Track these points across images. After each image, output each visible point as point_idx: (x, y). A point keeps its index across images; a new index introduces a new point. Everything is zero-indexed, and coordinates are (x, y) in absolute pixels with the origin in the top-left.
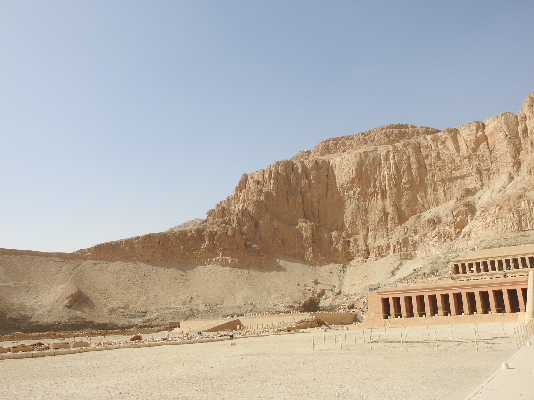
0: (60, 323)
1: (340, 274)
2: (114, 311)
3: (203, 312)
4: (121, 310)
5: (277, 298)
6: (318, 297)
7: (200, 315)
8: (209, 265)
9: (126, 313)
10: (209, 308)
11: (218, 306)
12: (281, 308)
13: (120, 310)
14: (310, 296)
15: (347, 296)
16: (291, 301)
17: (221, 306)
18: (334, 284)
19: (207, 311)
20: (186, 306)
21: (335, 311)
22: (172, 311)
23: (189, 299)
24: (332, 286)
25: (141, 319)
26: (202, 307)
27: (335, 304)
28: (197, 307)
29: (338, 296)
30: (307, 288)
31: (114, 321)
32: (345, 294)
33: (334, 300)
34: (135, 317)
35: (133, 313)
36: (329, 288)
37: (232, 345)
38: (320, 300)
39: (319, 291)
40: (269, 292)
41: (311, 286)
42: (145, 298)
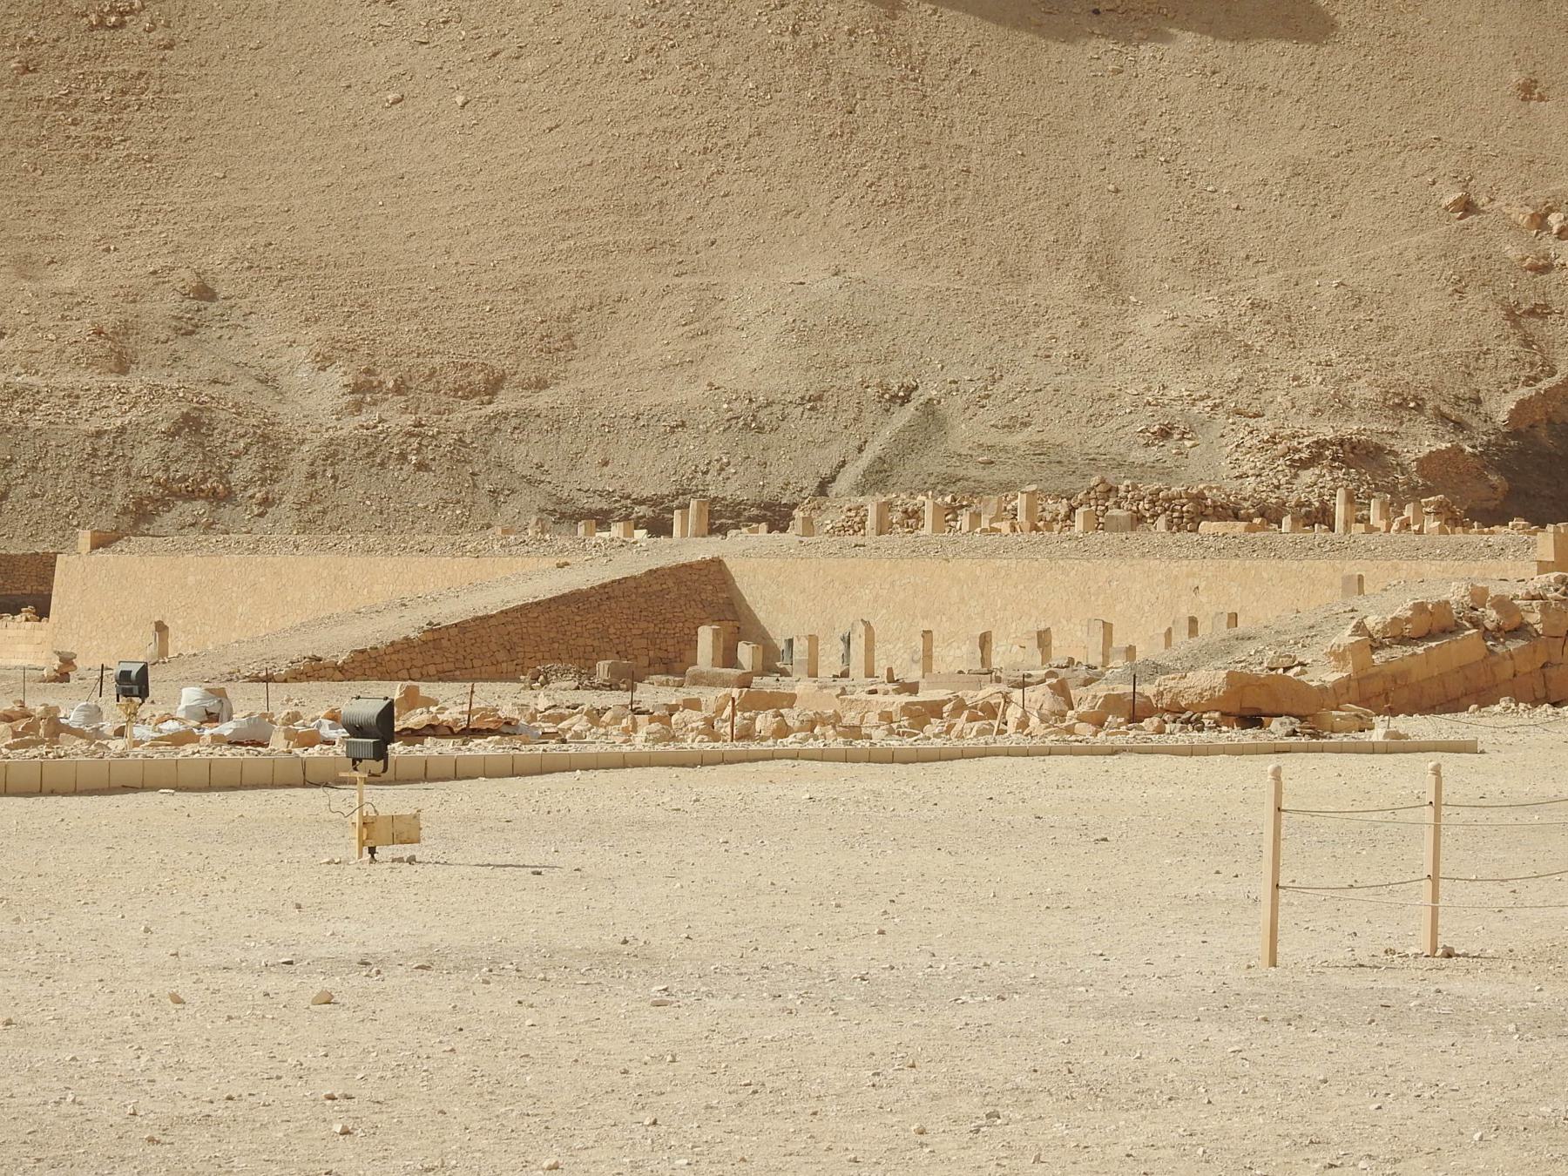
5: (1198, 345)
7: (293, 485)
10: (393, 416)
11: (506, 401)
12: (1225, 462)
16: (1363, 390)
17: (542, 400)
19: (373, 452)
20: (136, 382)
23: (166, 304)
28: (266, 400)
37: (375, 836)
40: (1109, 277)
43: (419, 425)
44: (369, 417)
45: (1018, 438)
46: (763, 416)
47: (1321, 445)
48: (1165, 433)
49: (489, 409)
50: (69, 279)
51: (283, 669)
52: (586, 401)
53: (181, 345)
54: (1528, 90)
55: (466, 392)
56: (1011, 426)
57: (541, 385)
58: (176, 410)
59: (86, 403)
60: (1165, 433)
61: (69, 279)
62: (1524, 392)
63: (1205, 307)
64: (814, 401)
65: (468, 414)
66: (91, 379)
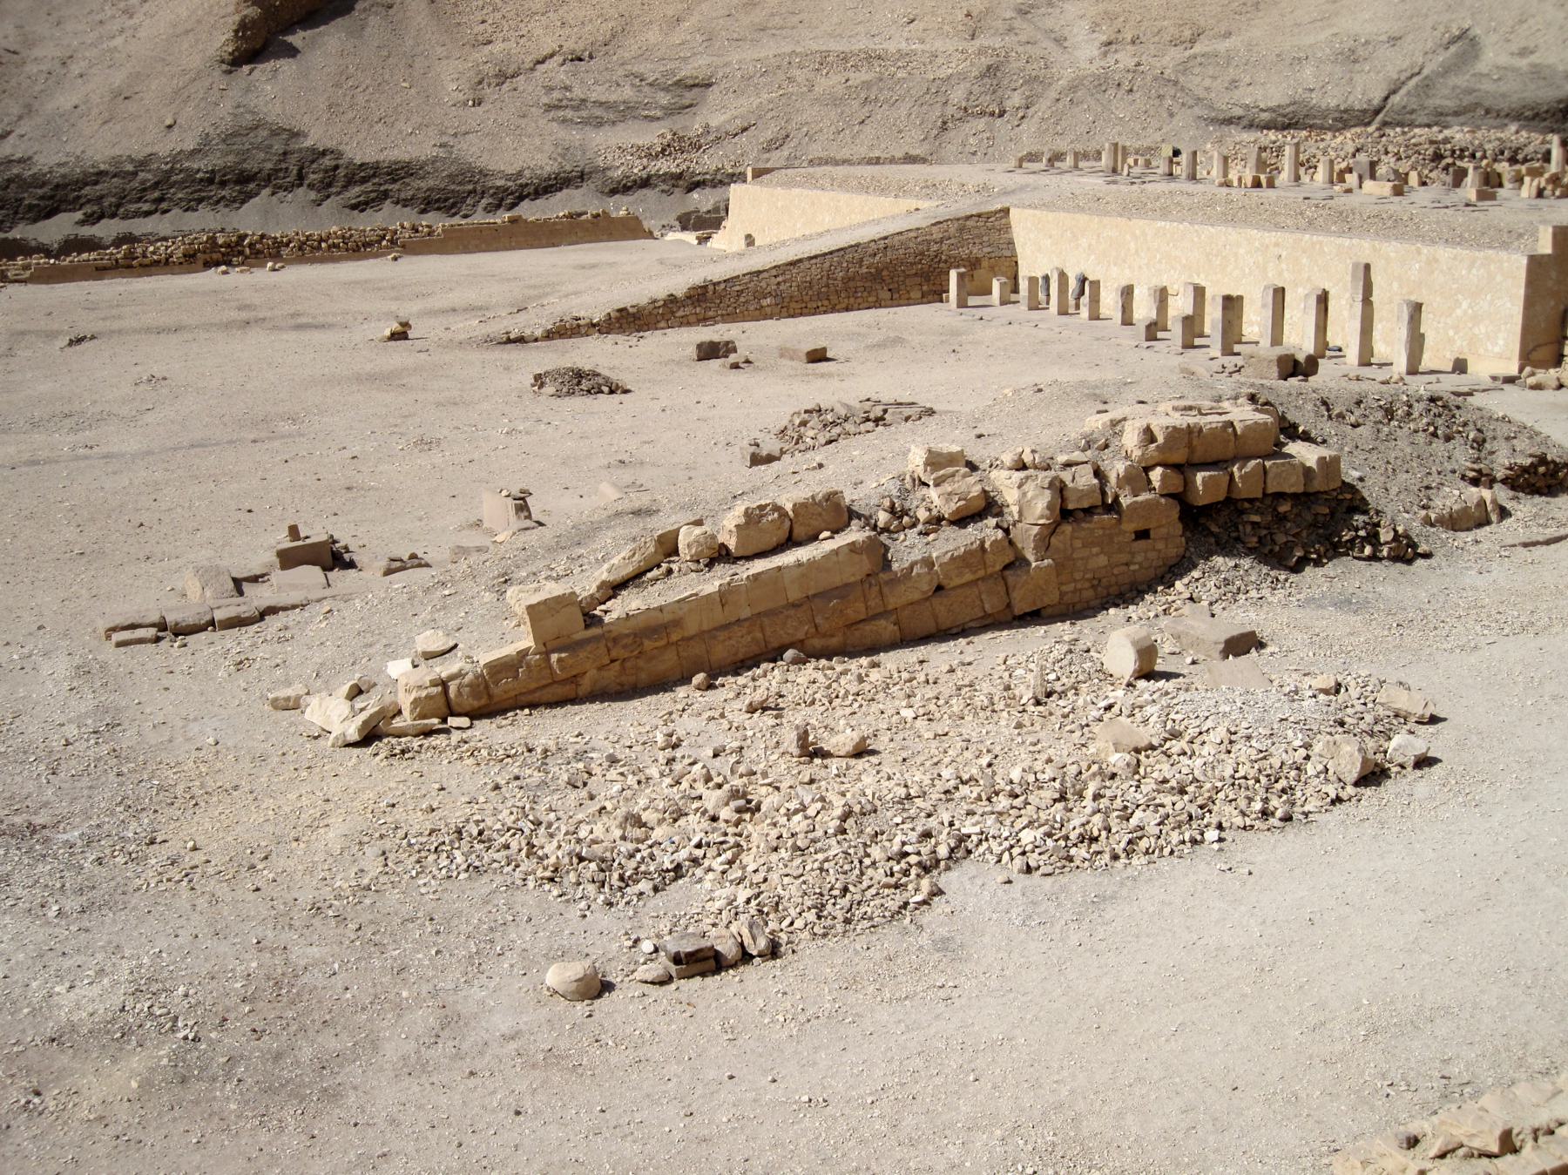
0: (143, 164)
2: (503, 77)
3: (1073, 88)
4: (555, 72)
9: (578, 92)
13: (555, 72)
17: (1223, 46)
25: (652, 136)
26: (1085, 53)
34: (625, 113)
35: (627, 93)
43: (1138, 64)
44: (1111, 60)
45: (1523, 63)
46: (1360, 52)
49: (1187, 53)
51: (539, 333)
52: (1250, 47)
53: (1017, 23)
55: (1174, 43)
56: (1524, 52)
57: (1228, 35)
58: (985, 61)
59: (940, 60)
64: (1394, 40)
65: (1176, 55)
66: (950, 46)
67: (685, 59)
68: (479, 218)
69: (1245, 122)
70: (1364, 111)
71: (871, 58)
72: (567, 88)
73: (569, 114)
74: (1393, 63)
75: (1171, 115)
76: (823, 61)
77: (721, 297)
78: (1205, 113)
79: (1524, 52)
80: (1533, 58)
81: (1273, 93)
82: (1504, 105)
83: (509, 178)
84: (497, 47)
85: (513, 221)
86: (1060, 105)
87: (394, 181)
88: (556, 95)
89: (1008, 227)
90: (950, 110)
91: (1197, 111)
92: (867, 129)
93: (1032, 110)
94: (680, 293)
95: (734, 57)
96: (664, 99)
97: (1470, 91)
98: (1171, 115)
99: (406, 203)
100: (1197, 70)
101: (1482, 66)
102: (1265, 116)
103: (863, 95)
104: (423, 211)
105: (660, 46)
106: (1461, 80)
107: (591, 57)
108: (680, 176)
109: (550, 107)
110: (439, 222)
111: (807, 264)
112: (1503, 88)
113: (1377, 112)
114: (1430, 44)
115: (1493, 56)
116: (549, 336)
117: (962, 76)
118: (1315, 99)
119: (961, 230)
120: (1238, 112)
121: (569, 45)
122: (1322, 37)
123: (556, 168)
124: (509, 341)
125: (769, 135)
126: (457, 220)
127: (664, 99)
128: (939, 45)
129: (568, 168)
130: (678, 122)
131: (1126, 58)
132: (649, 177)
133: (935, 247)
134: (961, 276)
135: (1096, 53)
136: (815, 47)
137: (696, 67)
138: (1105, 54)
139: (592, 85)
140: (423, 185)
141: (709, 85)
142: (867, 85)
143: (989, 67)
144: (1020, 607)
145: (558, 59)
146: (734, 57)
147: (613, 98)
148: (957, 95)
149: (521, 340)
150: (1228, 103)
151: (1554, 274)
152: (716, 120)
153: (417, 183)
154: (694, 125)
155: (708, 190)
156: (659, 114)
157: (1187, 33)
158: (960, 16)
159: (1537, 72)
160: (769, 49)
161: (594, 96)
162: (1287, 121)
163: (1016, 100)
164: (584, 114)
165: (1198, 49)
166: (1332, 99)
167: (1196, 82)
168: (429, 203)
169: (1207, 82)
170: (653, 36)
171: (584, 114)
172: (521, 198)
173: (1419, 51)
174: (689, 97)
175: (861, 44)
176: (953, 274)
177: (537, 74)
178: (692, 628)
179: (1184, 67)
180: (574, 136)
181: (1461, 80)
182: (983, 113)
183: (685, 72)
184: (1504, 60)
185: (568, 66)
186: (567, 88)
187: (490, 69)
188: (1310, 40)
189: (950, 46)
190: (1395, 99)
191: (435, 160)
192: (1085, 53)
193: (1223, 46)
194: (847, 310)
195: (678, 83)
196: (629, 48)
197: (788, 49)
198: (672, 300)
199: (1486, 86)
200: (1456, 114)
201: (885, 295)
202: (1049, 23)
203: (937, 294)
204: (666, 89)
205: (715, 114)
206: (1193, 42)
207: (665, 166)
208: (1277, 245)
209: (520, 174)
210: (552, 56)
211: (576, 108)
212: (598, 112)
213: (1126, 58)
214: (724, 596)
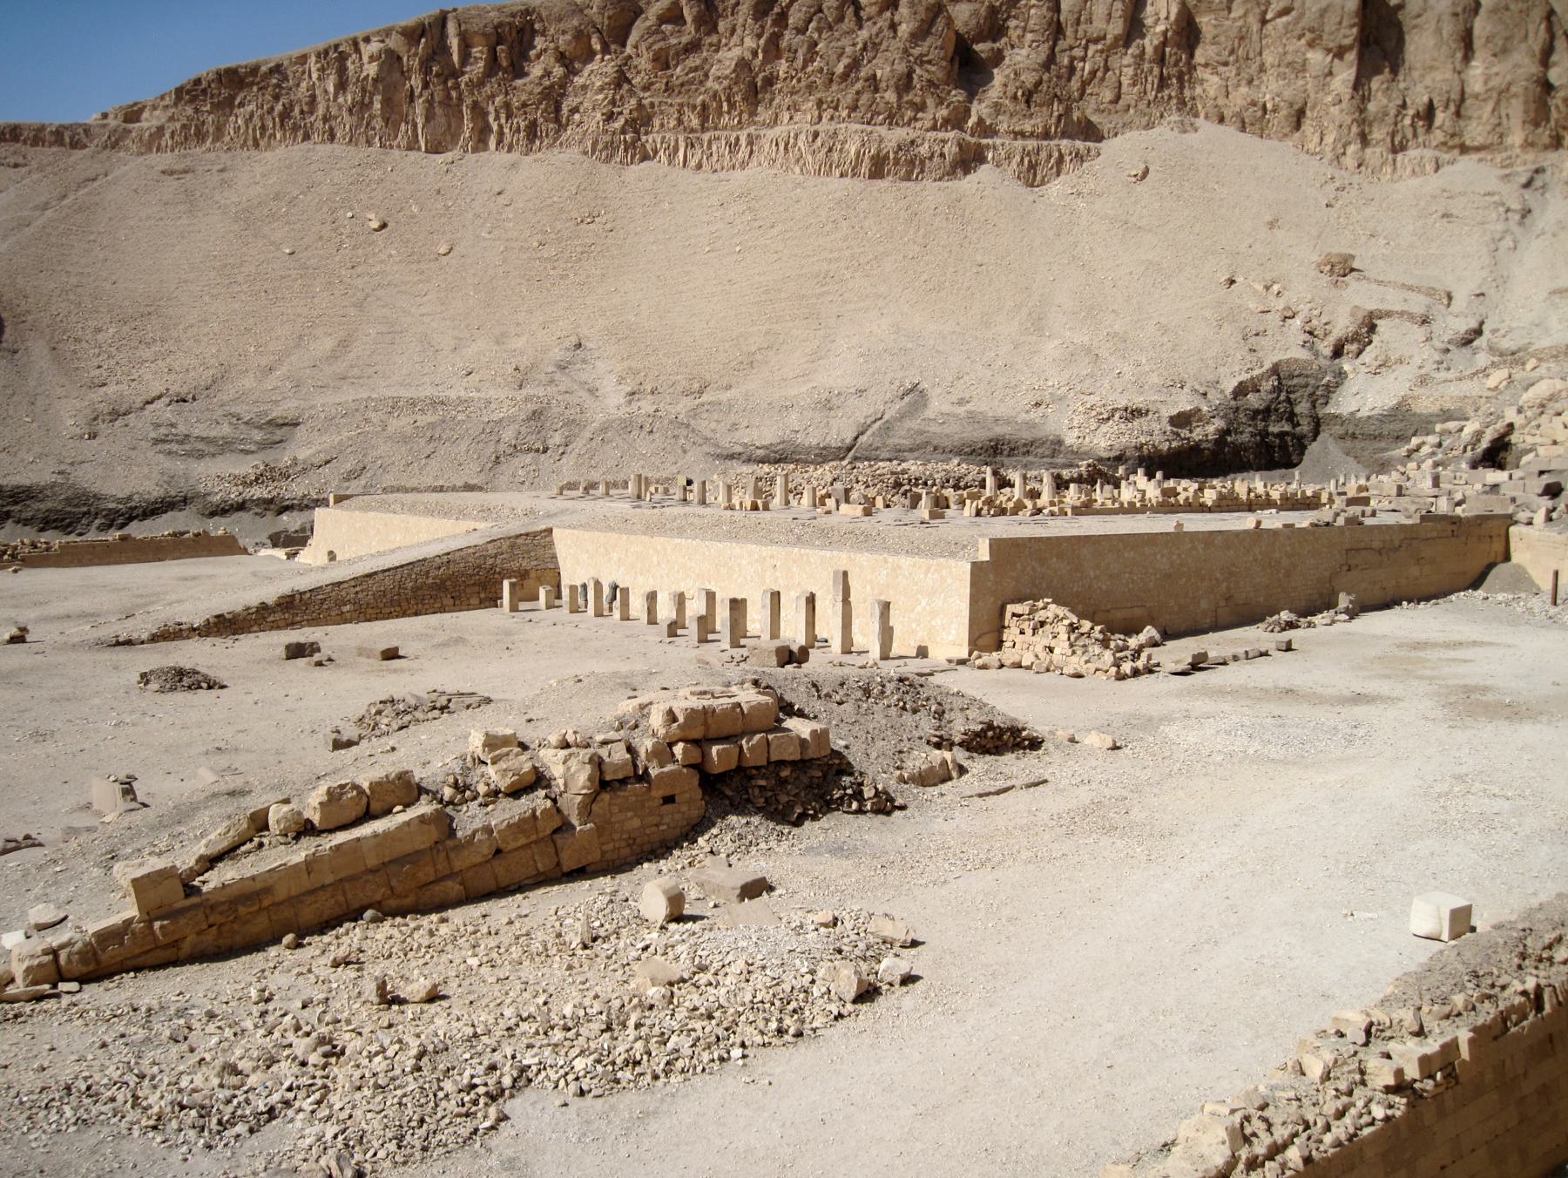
1: (1500, 227)
2: (115, 415)
3: (604, 429)
4: (163, 411)
6: (1338, 352)
8: (744, 165)
9: (182, 429)
14: (1287, 347)
15: (1514, 357)
16: (1155, 379)
17: (725, 396)
18: (1449, 283)
21: (1383, 467)
22: (423, 420)
24: (1431, 292)
25: (247, 467)
26: (613, 401)
27: (1426, 404)
29: (1457, 354)
30: (1280, 304)
31: (90, 478)
32: (1506, 344)
33: (1423, 381)
34: (224, 446)
35: (226, 430)
36: (1418, 304)
38: (1341, 375)
39: (1343, 325)
40: (1038, 324)
41: (1305, 289)
42: (328, 344)
44: (635, 406)
45: (961, 410)
46: (834, 401)
47: (1115, 410)
48: (1038, 404)
49: (697, 401)
50: (519, 343)
51: (145, 636)
52: (746, 397)
53: (558, 376)
54: (1272, 225)
56: (961, 402)
57: (729, 387)
58: (531, 407)
59: (493, 406)
60: (1038, 404)
61: (519, 343)
62: (1245, 377)
63: (1081, 338)
64: (861, 392)
65: (686, 404)
66: (502, 394)
67: (276, 402)
68: (93, 536)
69: (744, 457)
70: (839, 448)
71: (435, 403)
72: (172, 425)
73: (174, 447)
74: (861, 411)
75: (685, 452)
76: (395, 406)
77: (306, 605)
78: (711, 450)
79: (961, 402)
80: (968, 407)
81: (766, 435)
82: (947, 443)
83: (119, 501)
84: (111, 389)
85: (123, 539)
86: (593, 443)
87: (16, 503)
88: (163, 430)
89: (552, 544)
90: (502, 447)
91: (706, 449)
92: (433, 462)
93: (569, 449)
94: (271, 600)
95: (319, 401)
96: (258, 436)
97: (921, 433)
98: (685, 452)
99: (26, 522)
100: (705, 415)
101: (930, 413)
102: (761, 452)
103: (429, 434)
104: (42, 530)
105: (254, 391)
106: (914, 424)
107: (194, 399)
108: (271, 501)
109: (157, 441)
110: (56, 539)
111: (381, 576)
112: (947, 430)
113: (849, 449)
114: (889, 395)
115: (938, 405)
116: (154, 639)
117: (512, 419)
118: (800, 438)
119: (512, 546)
120: (738, 449)
121: (175, 389)
122: (804, 389)
123: (162, 493)
124: (118, 644)
125: (349, 467)
126: (72, 538)
127: (258, 436)
128: (492, 393)
129: (173, 493)
130: (270, 456)
131: (646, 405)
132: (244, 502)
133: (491, 561)
134: (512, 585)
135: (622, 401)
136: (388, 393)
137: (286, 408)
138: (630, 402)
139: (195, 423)
140: (42, 506)
141: (297, 424)
142: (432, 426)
143: (534, 412)
144: (567, 865)
145: (165, 400)
146: (319, 401)
147: (213, 434)
148: (508, 435)
149: (129, 643)
150: (727, 442)
151: (991, 577)
152: (303, 454)
153: (37, 505)
154: (284, 458)
155: (295, 513)
156: (253, 448)
157: (696, 386)
158: (510, 370)
159: (972, 417)
160: (348, 395)
161: (196, 432)
162: (778, 456)
163: (557, 439)
164: (187, 447)
165: (705, 398)
166: (813, 439)
167: (704, 425)
168: (46, 523)
169: (713, 425)
170: (248, 382)
171: (187, 447)
172: (131, 519)
173: (880, 402)
174: (279, 434)
175: (428, 392)
176: (506, 584)
177: (146, 412)
178: (281, 893)
179: (694, 413)
180: (178, 466)
181: (914, 424)
182: (529, 450)
183: (275, 413)
184: (946, 408)
185: (174, 406)
186: (172, 425)
187: (105, 408)
188: (793, 392)
189: (502, 394)
190: (863, 439)
191: (53, 485)
192: (613, 401)
193: (725, 396)
194: (416, 614)
195: (270, 422)
196: (228, 392)
197: (365, 395)
198: (263, 607)
199: (934, 428)
200: (911, 450)
201: (448, 601)
202: (583, 377)
203: (493, 601)
204: (260, 427)
205: (302, 448)
206: (701, 392)
207: (258, 492)
208: (772, 557)
209: (130, 498)
210: (159, 397)
211: (181, 443)
212: (200, 446)
213: (646, 405)
214: (310, 865)
